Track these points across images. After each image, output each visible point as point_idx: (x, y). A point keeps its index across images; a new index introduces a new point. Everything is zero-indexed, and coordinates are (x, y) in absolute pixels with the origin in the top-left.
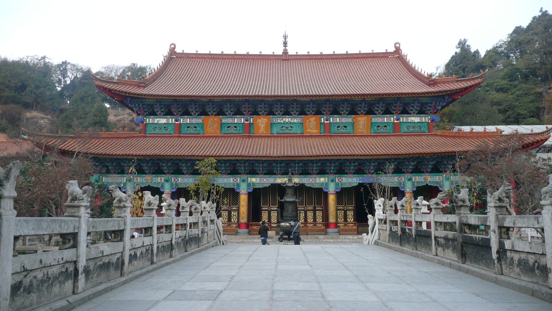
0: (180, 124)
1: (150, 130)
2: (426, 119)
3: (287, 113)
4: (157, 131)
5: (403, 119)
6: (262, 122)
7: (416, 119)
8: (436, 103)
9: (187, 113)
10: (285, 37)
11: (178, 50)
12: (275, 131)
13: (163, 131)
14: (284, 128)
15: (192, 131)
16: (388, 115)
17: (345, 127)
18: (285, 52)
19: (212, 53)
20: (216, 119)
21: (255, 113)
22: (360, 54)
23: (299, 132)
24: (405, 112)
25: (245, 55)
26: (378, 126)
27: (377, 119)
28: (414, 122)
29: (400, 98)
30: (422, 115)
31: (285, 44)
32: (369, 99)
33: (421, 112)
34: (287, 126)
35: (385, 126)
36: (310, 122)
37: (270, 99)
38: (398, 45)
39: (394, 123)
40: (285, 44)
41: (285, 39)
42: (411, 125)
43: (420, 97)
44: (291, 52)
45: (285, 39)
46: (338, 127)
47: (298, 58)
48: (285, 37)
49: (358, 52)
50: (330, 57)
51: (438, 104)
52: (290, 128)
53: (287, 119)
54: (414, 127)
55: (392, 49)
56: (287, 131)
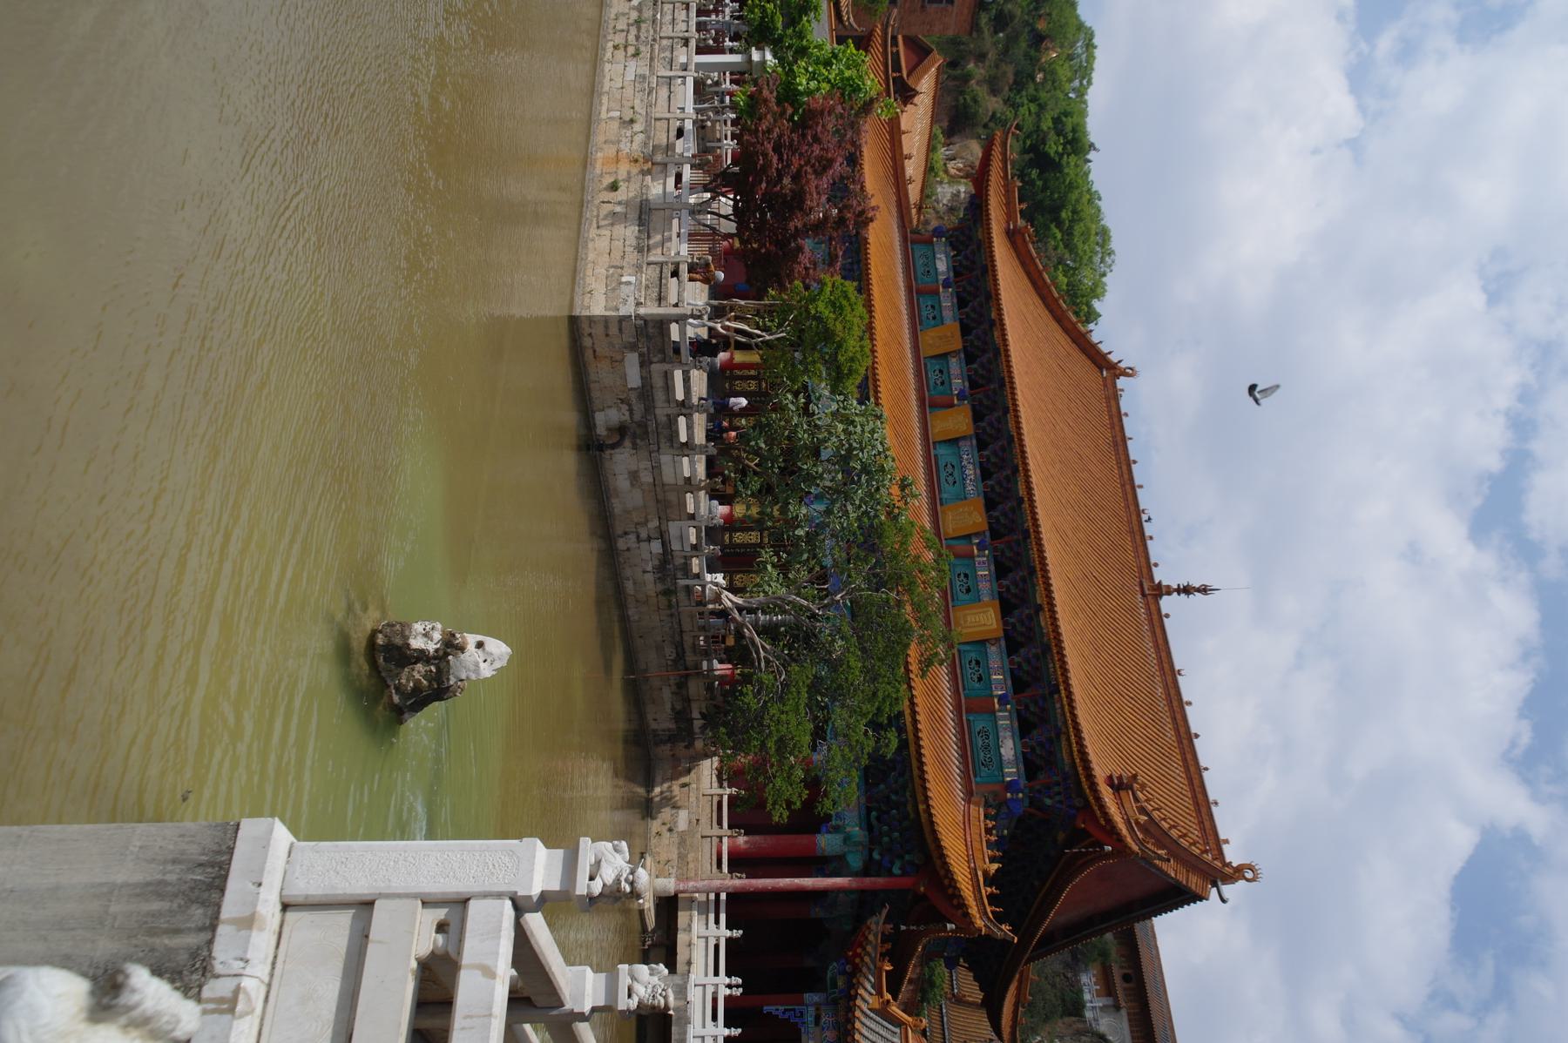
0: (937, 293)
1: (920, 250)
2: (1011, 772)
3: (985, 474)
4: (920, 262)
5: (1004, 719)
6: (958, 421)
7: (1008, 749)
8: (1058, 784)
9: (961, 303)
10: (1204, 590)
11: (1122, 382)
12: (943, 451)
13: (920, 270)
14: (950, 469)
15: (924, 313)
16: (1009, 682)
17: (968, 590)
18: (1160, 591)
19: (1129, 443)
20: (957, 343)
21: (977, 417)
22: (1199, 770)
23: (945, 496)
24: (1024, 728)
25: (1137, 505)
26: (978, 663)
27: (995, 656)
28: (999, 747)
29: (1059, 692)
30: (1021, 766)
31: (1187, 590)
32: (1044, 619)
33: (1030, 765)
34: (956, 473)
35: (980, 679)
36: (970, 514)
37: (1011, 424)
38: (1249, 875)
39: (992, 697)
40: (1187, 590)
41: (1198, 590)
42: (991, 741)
43: (1068, 739)
44: (1166, 603)
45: (1198, 590)
46: (966, 576)
47: (1157, 622)
48: (1204, 590)
49: (1203, 764)
50: (1172, 692)
51: (1056, 789)
52: (950, 479)
53: (971, 472)
54: (986, 748)
55: (1233, 855)
56: (943, 475)
